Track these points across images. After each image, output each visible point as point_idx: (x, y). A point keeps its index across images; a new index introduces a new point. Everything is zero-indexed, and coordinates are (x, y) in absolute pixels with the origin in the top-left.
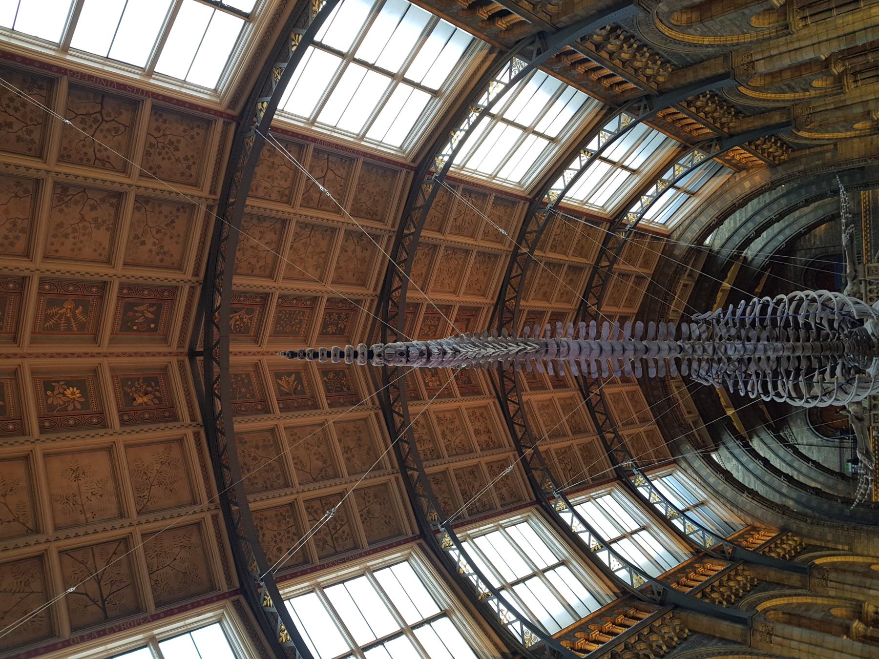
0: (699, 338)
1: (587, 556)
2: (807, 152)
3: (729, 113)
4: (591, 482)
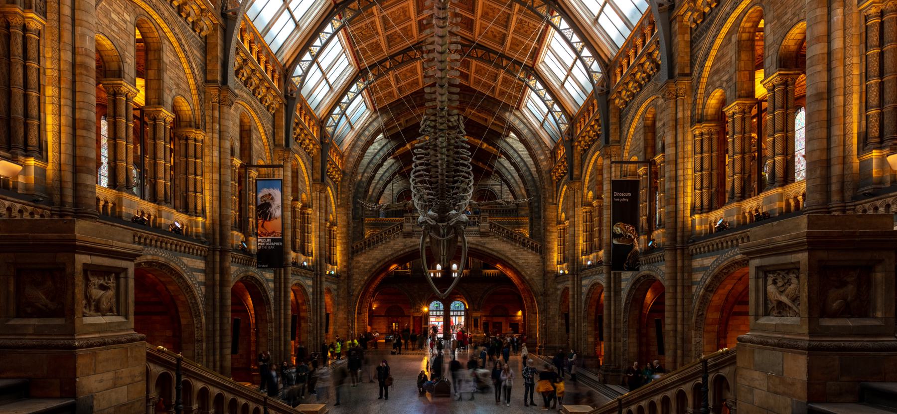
1: (305, 45)
3: (585, 146)
4: (355, 49)
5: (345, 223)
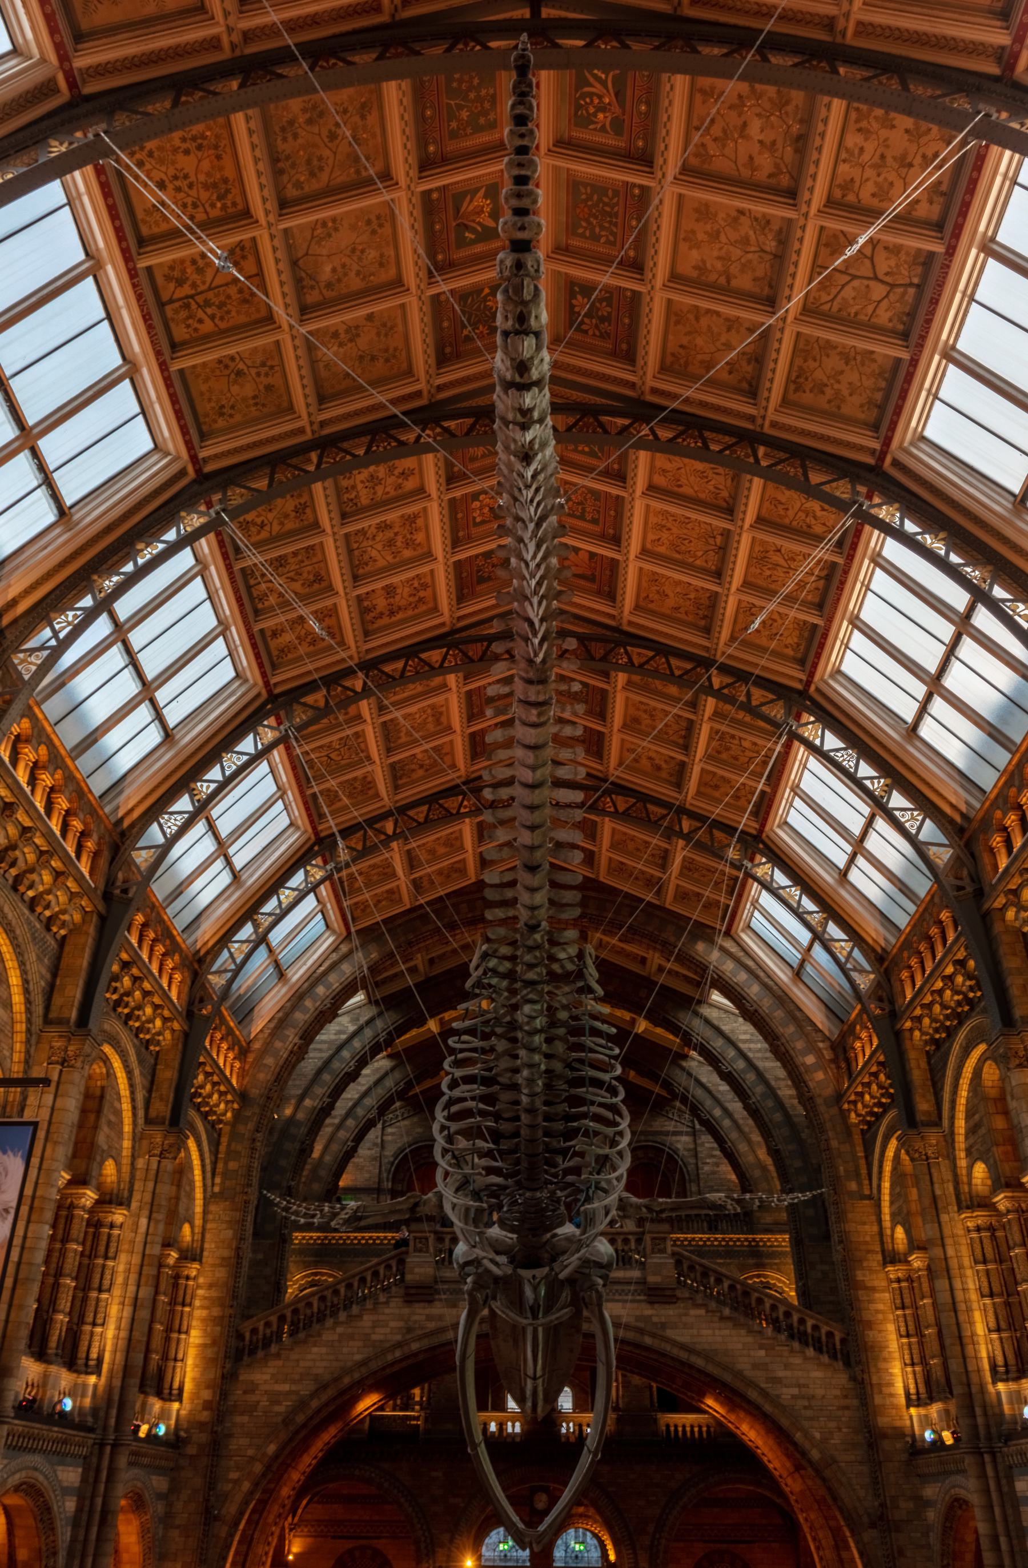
0: (552, 958)
2: (861, 1154)
4: (309, 792)
5: (226, 1253)
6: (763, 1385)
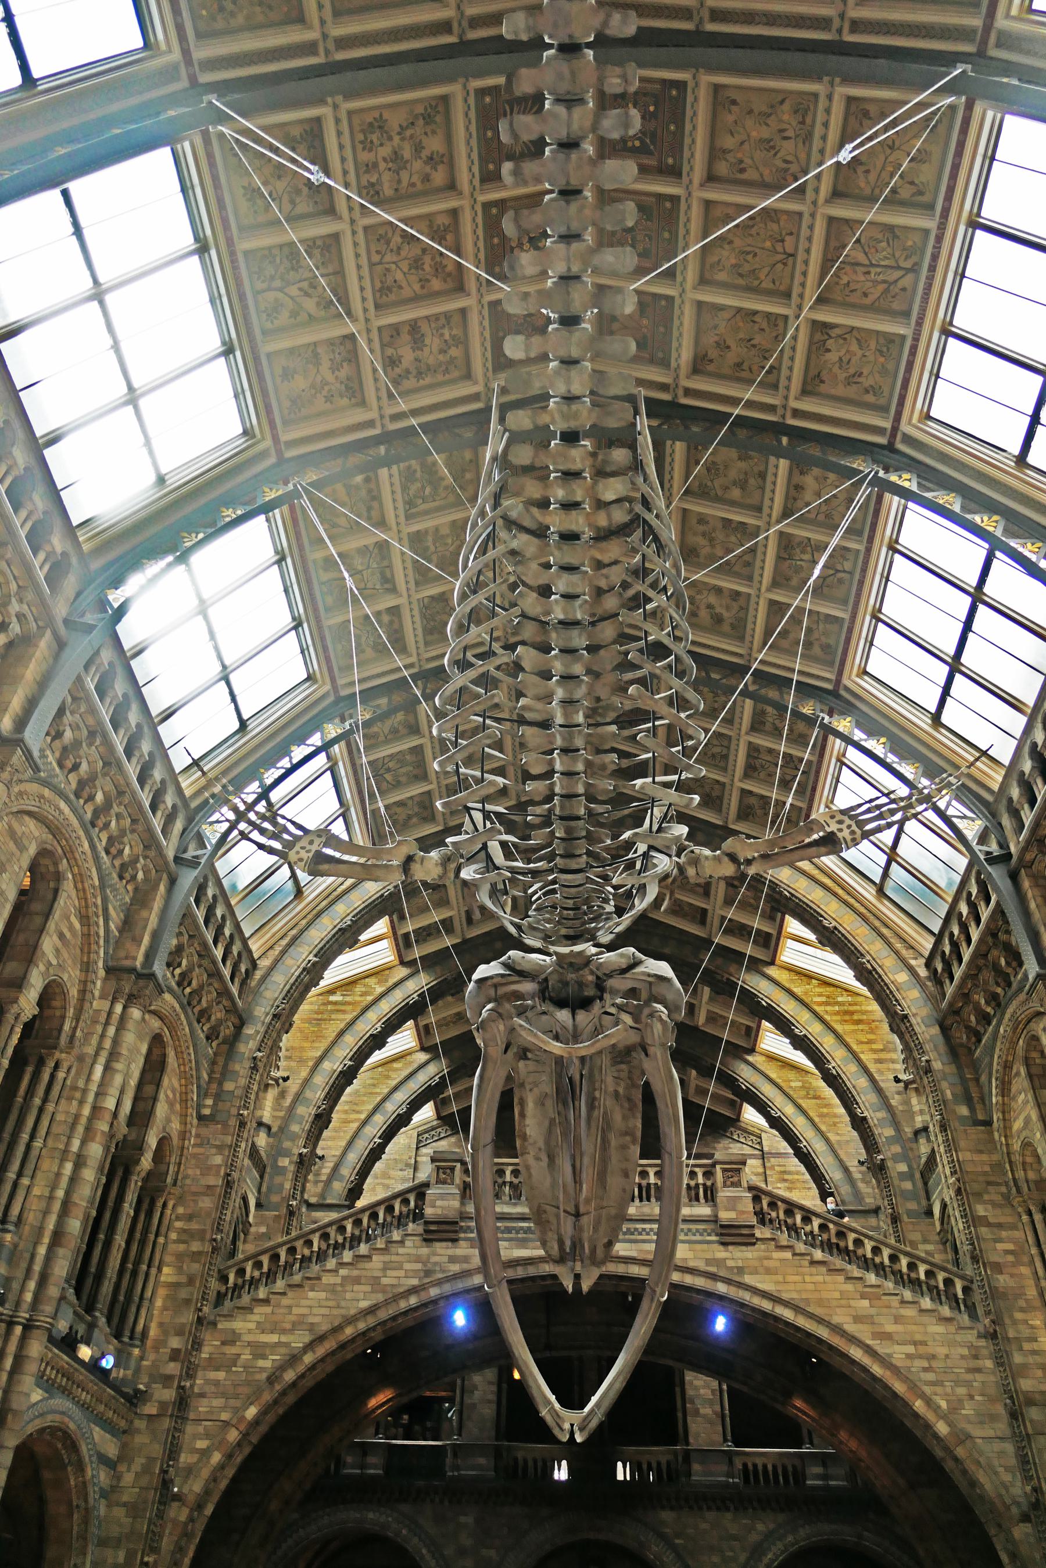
6: (869, 1342)
